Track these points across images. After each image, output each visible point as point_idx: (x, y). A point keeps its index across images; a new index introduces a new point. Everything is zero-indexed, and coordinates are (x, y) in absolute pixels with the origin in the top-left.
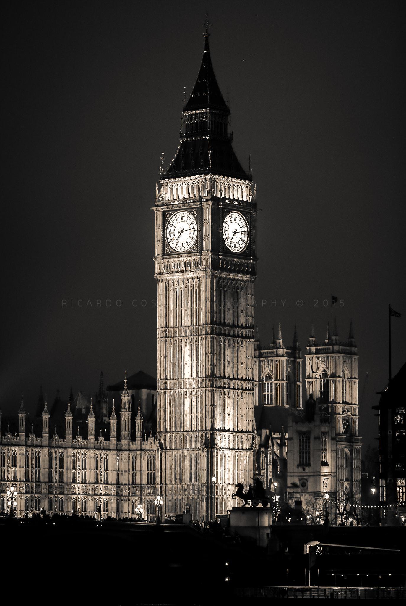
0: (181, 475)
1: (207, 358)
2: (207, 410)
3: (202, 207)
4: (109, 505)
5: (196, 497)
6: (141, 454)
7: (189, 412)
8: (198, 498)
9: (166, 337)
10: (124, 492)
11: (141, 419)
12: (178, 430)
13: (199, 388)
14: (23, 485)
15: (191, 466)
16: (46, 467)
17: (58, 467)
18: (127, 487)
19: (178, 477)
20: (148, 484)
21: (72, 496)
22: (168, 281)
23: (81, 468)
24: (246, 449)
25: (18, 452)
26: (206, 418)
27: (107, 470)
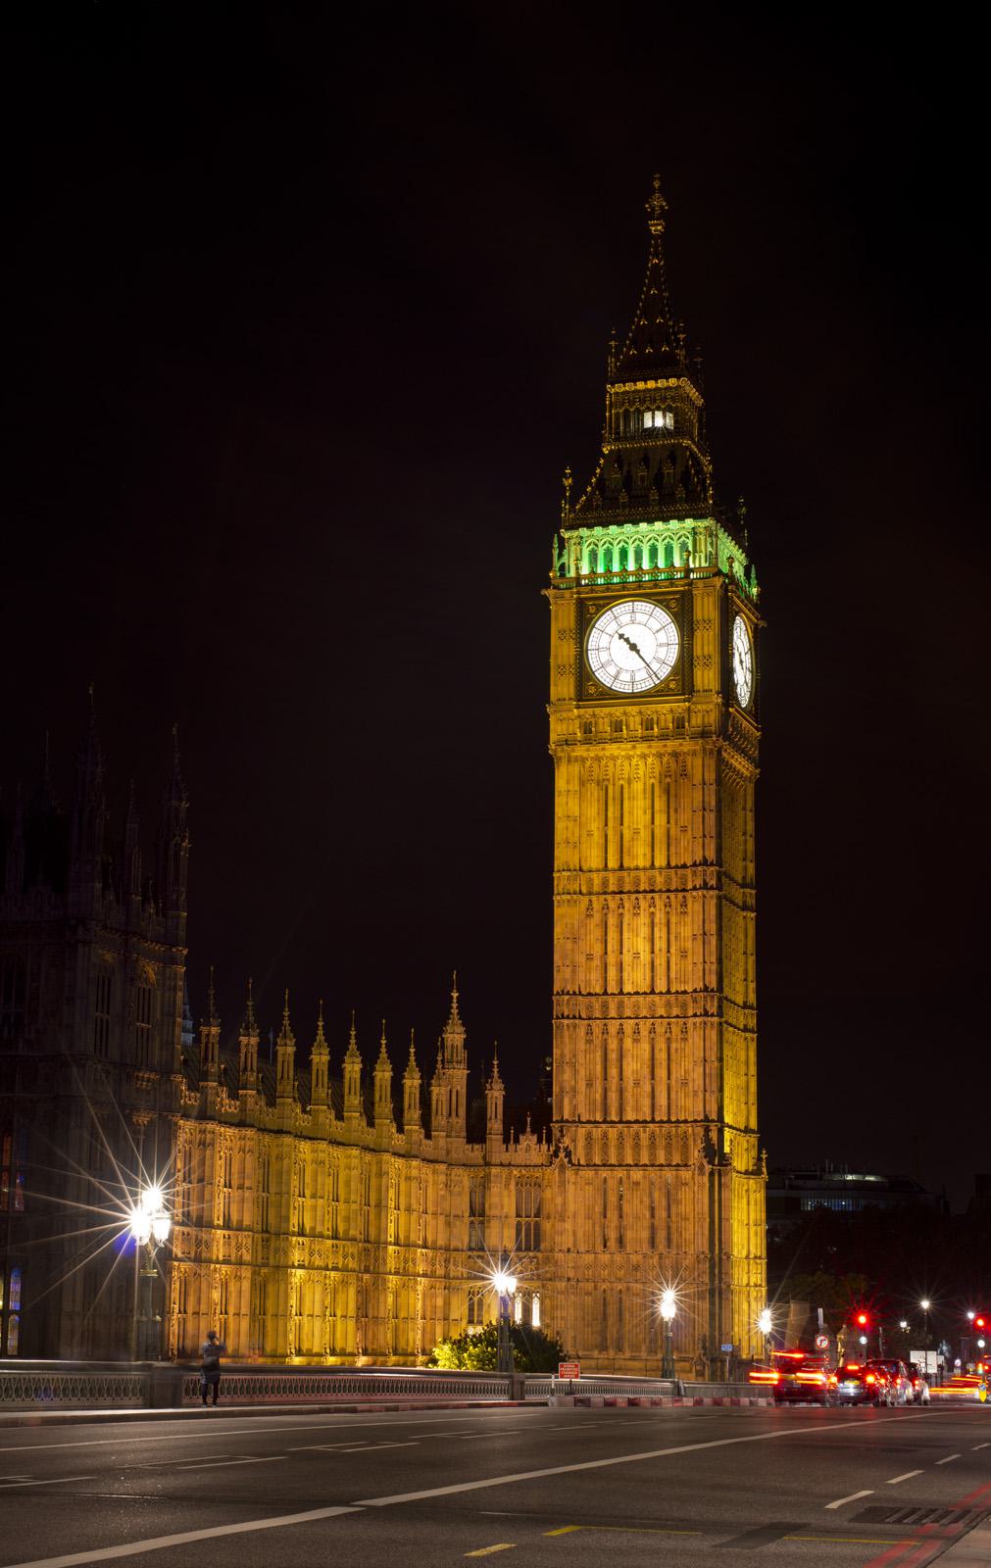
0: (621, 1229)
2: (707, 1071)
7: (648, 1076)
9: (581, 893)
10: (452, 1267)
13: (677, 1017)
15: (652, 1209)
20: (519, 1249)
22: (583, 760)
24: (747, 1172)
26: (705, 1091)
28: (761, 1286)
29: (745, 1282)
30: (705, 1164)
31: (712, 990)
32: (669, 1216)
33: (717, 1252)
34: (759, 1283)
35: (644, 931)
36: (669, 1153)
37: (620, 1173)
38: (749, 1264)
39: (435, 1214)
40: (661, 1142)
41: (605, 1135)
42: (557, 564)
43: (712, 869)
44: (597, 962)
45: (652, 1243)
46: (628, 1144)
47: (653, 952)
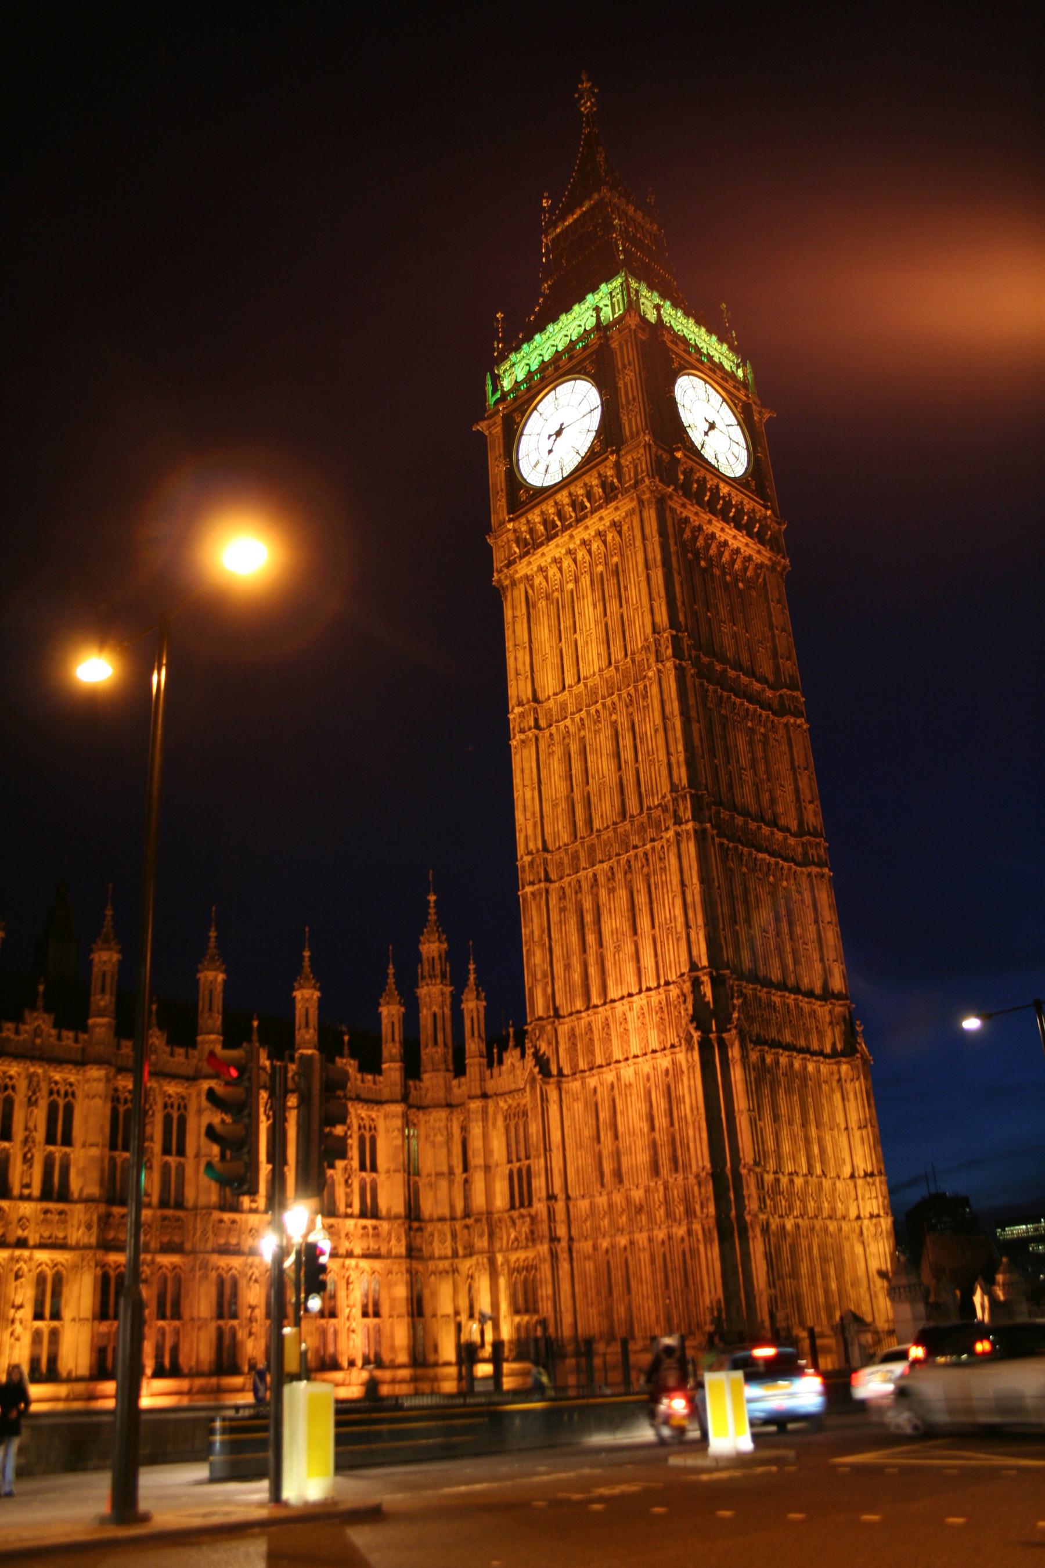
0: (617, 1155)
1: (670, 734)
2: (689, 899)
3: (608, 346)
5: (681, 1231)
6: (485, 1111)
8: (690, 1232)
10: (436, 1245)
11: (478, 998)
12: (596, 1000)
13: (653, 840)
15: (651, 1118)
16: (92, 1139)
18: (446, 1227)
19: (608, 1167)
20: (512, 1207)
21: (223, 1261)
22: (528, 579)
28: (878, 1216)
29: (853, 1214)
30: (692, 1031)
31: (684, 788)
32: (672, 1124)
34: (876, 1212)
37: (609, 1077)
38: (855, 1186)
39: (388, 1171)
41: (590, 1027)
42: (492, 400)
43: (665, 635)
44: (563, 805)
47: (620, 768)
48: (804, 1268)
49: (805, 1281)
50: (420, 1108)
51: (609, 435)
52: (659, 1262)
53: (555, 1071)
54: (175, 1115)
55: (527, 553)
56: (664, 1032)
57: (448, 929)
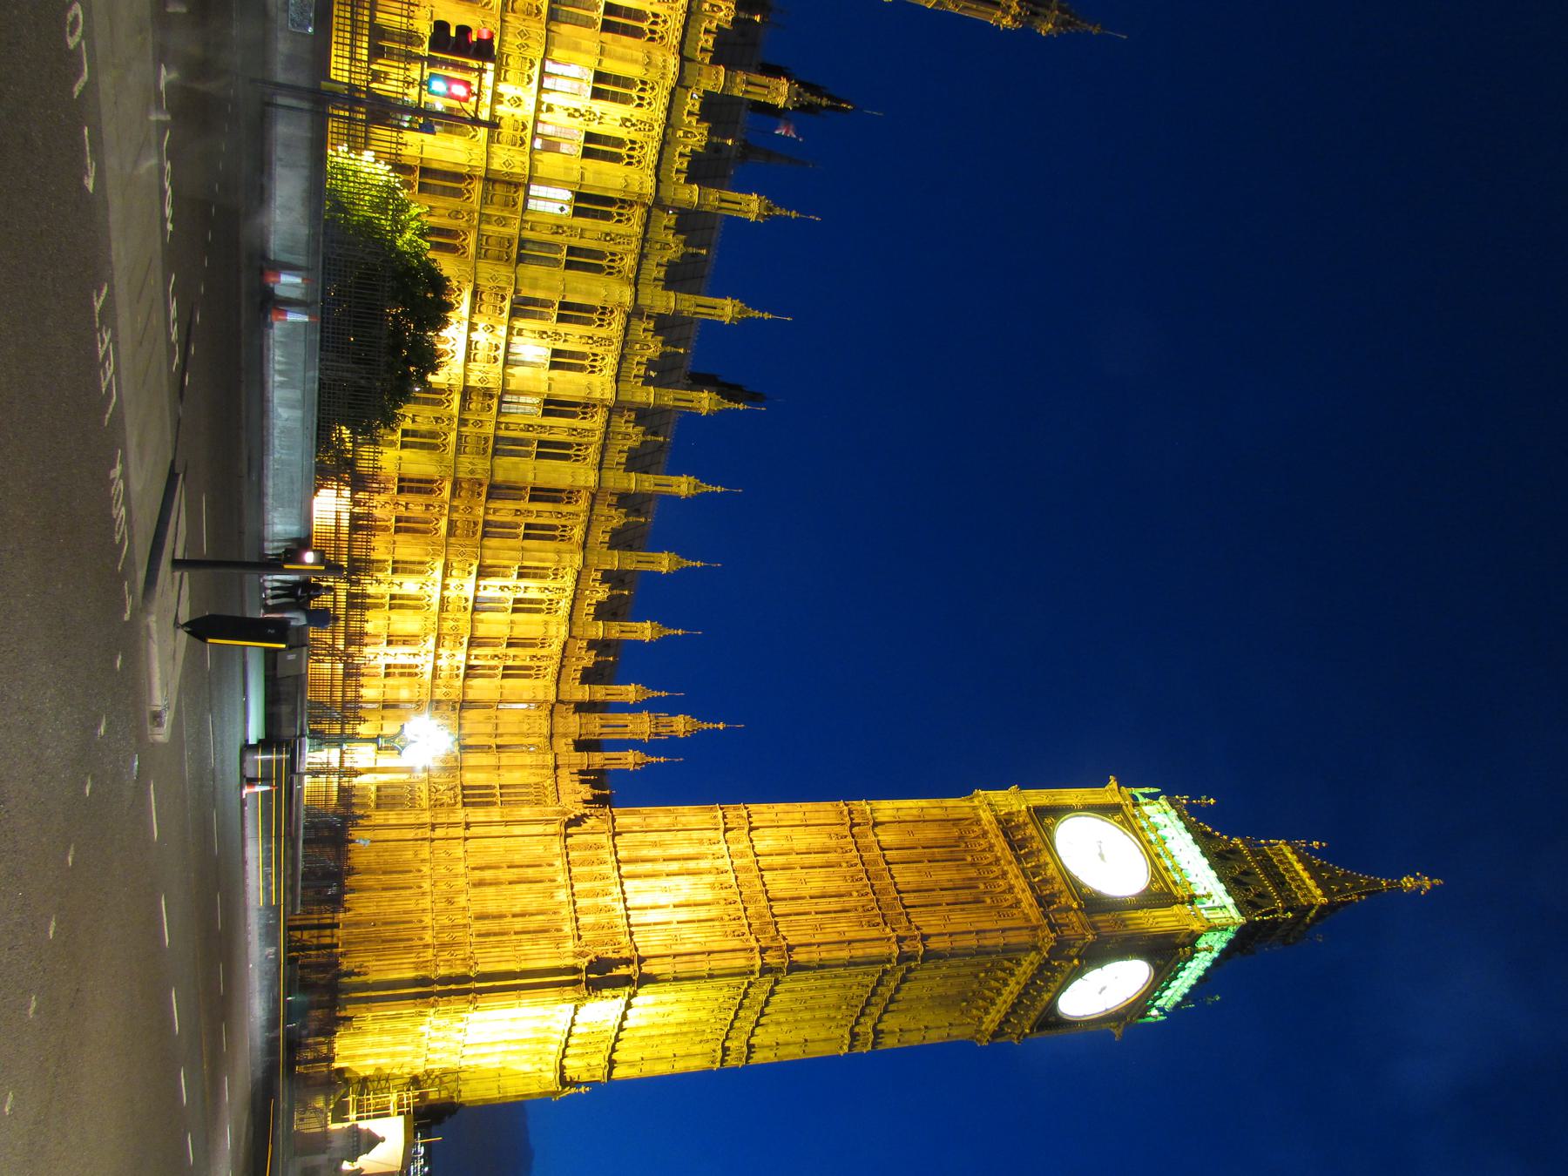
2: (698, 957)
4: (405, 680)
5: (428, 939)
6: (543, 767)
12: (625, 869)
13: (750, 925)
14: (494, 383)
15: (523, 915)
16: (540, 476)
17: (532, 520)
19: (488, 875)
20: (464, 788)
21: (439, 564)
23: (521, 595)
24: (562, 1068)
25: (595, 379)
26: (675, 956)
27: (504, 676)
33: (478, 985)
35: (832, 887)
36: (594, 927)
37: (562, 878)
40: (603, 918)
42: (1137, 792)
45: (481, 917)
46: (598, 885)
48: (386, 1038)
49: (376, 1039)
50: (552, 712)
51: (1094, 904)
52: (406, 917)
53: (570, 831)
54: (557, 533)
55: (999, 822)
56: (592, 929)
57: (697, 738)
